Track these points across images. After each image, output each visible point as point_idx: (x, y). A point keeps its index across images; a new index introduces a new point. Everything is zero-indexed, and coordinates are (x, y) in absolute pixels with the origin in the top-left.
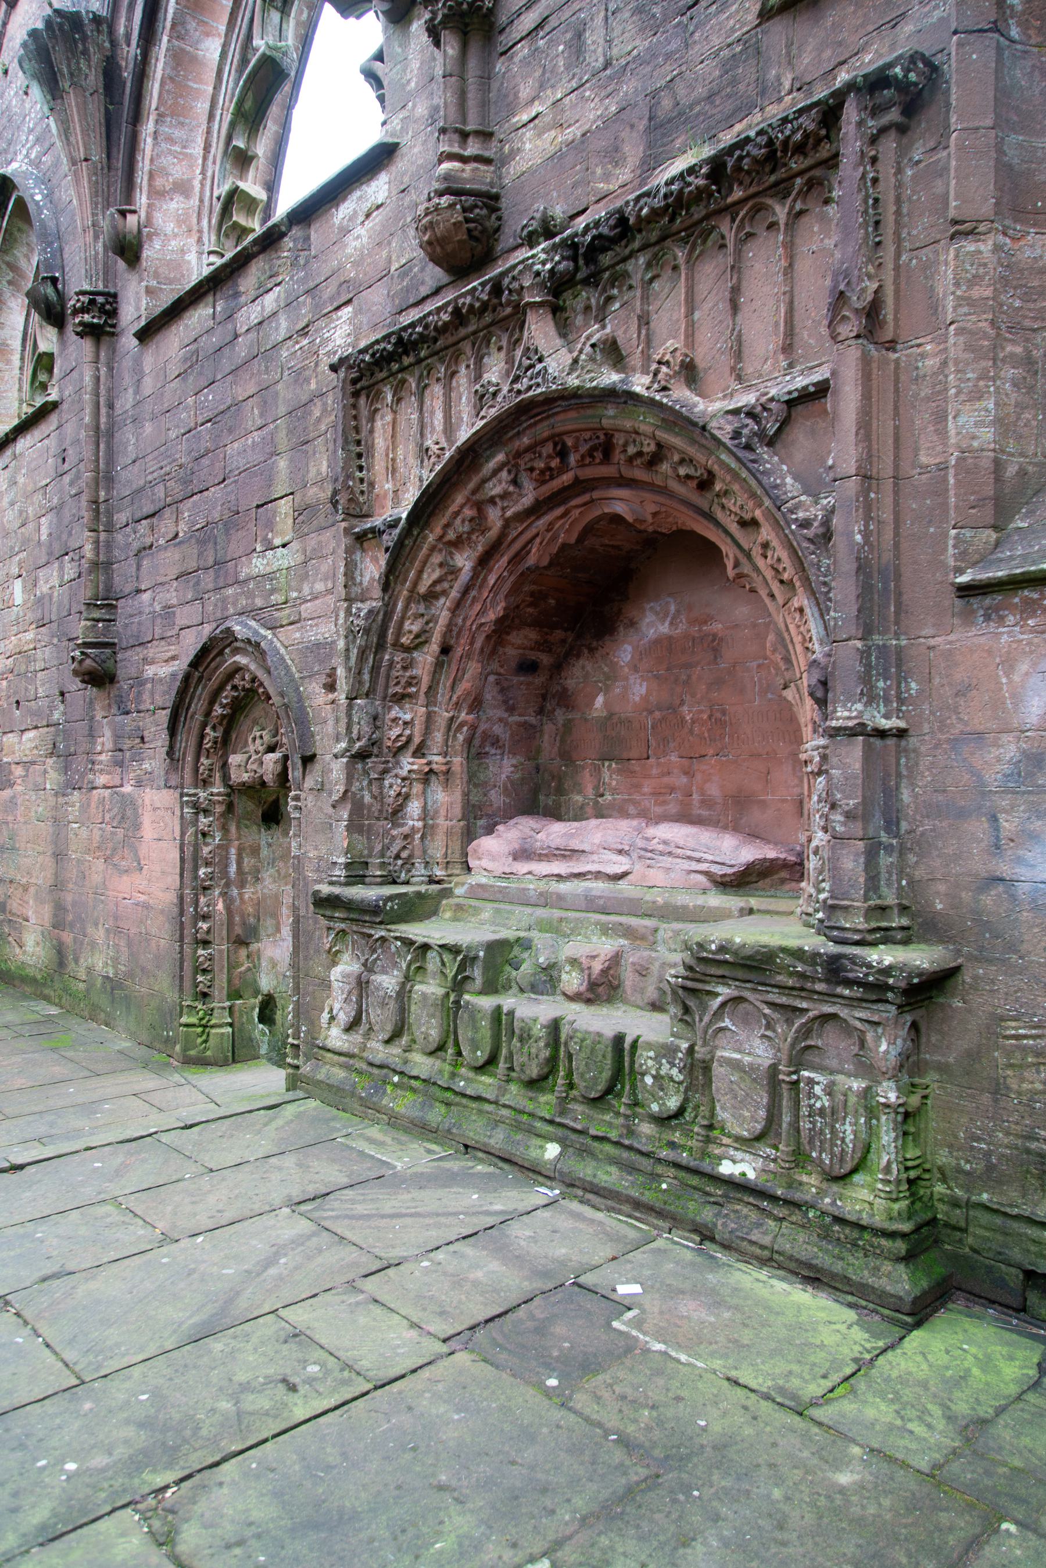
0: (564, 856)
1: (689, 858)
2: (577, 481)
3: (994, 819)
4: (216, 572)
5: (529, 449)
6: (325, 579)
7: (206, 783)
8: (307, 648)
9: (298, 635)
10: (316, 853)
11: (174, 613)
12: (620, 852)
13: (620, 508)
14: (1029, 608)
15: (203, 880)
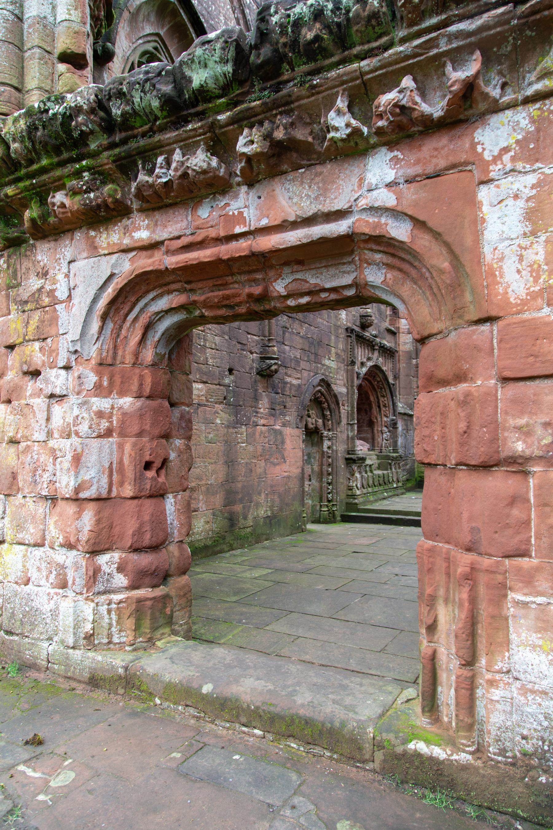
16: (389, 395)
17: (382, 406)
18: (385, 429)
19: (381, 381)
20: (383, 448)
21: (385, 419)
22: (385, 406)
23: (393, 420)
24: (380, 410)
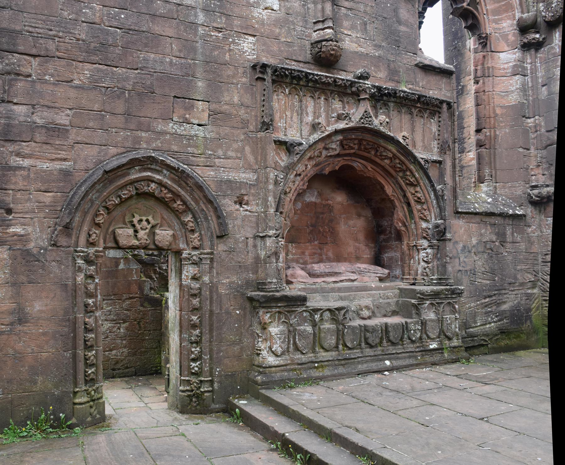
0: (331, 275)
1: (374, 273)
2: (354, 153)
3: (459, 259)
4: (126, 119)
5: (351, 139)
6: (237, 151)
7: (93, 244)
8: (221, 181)
9: (212, 173)
10: (228, 280)
11: (67, 131)
12: (353, 272)
13: (355, 165)
14: (463, 218)
15: (92, 307)
16: (424, 182)
17: (412, 202)
18: (425, 243)
19: (394, 155)
20: (419, 277)
21: (424, 225)
22: (419, 201)
23: (437, 226)
24: (411, 211)
